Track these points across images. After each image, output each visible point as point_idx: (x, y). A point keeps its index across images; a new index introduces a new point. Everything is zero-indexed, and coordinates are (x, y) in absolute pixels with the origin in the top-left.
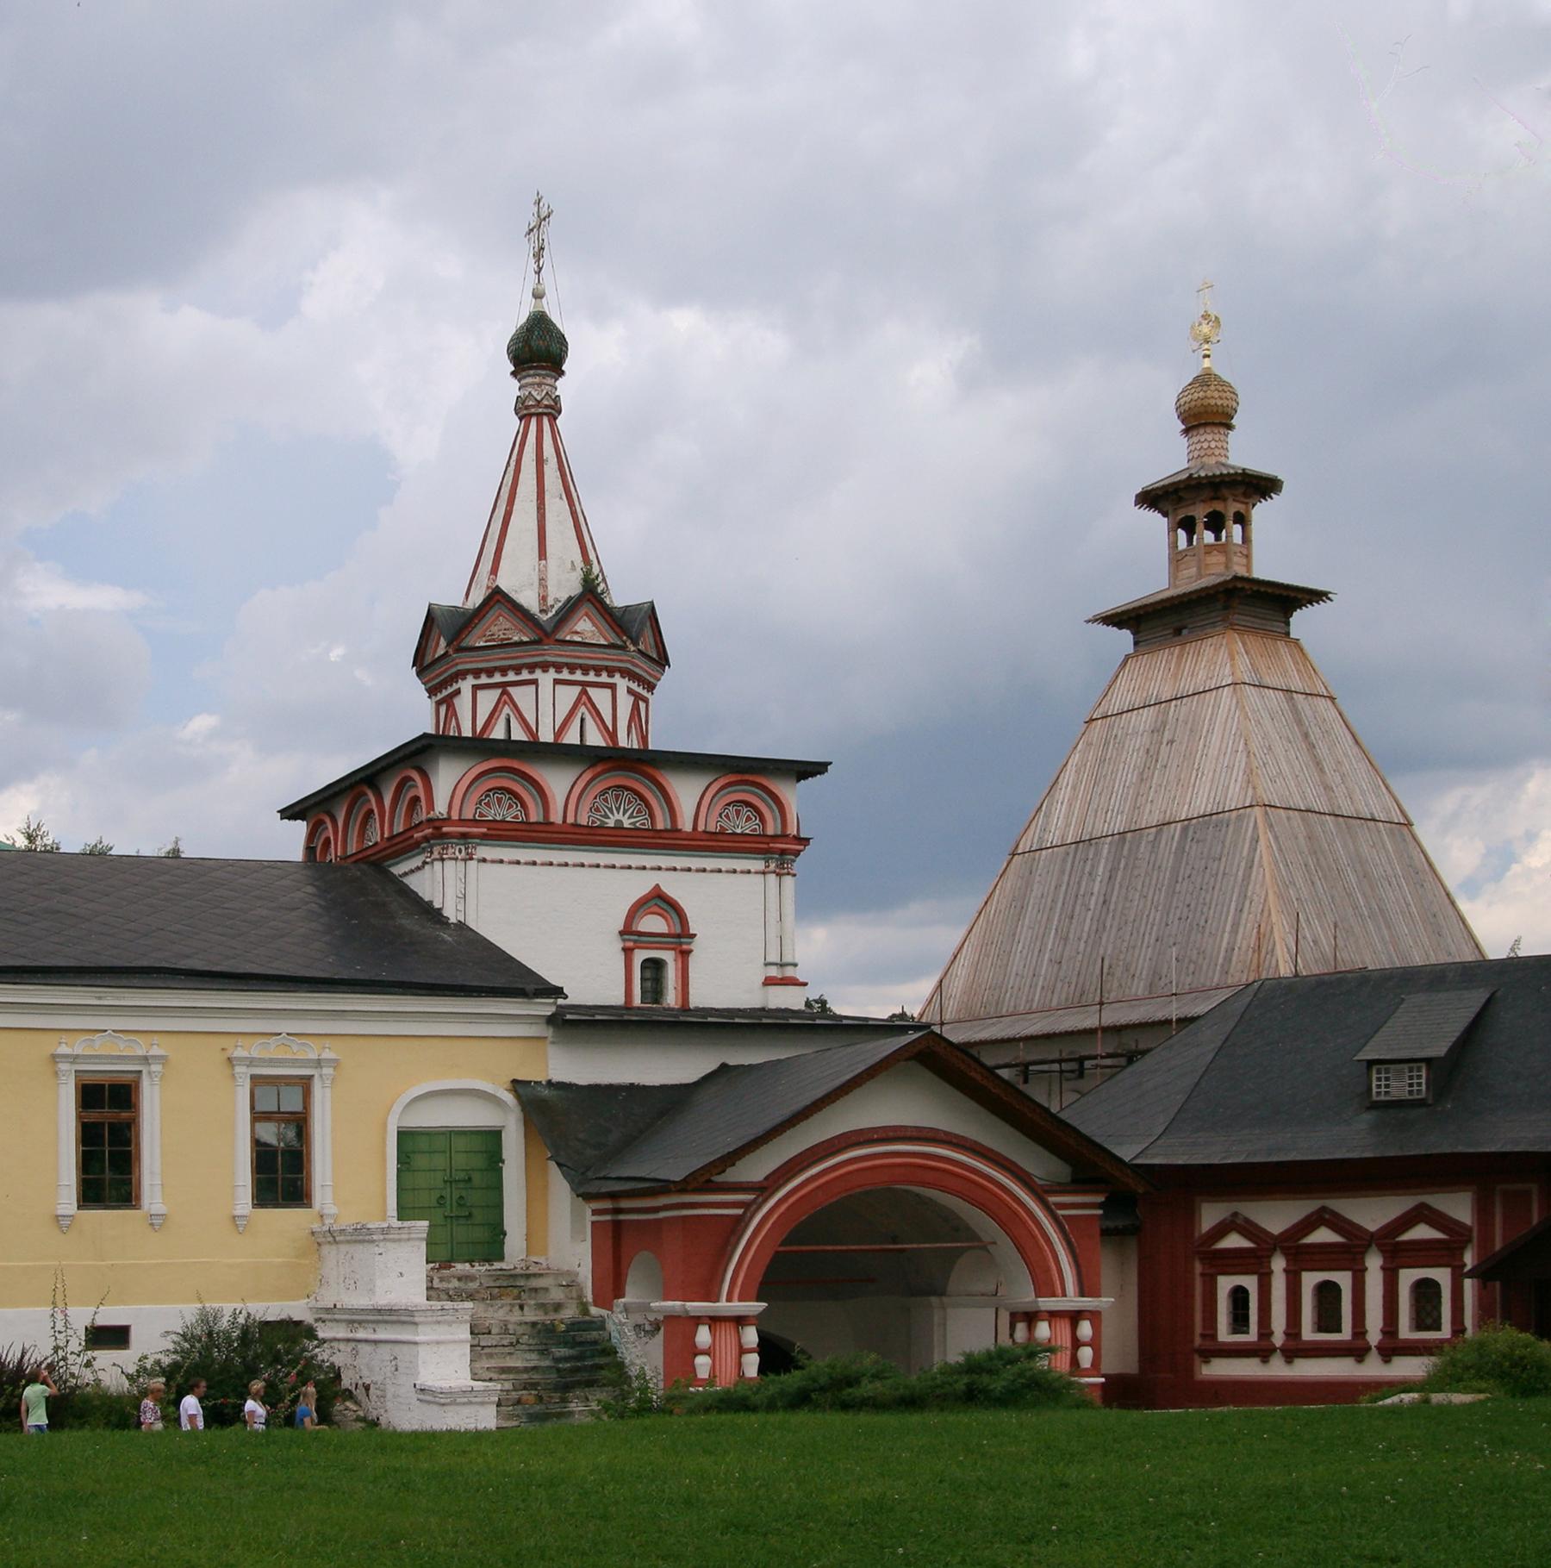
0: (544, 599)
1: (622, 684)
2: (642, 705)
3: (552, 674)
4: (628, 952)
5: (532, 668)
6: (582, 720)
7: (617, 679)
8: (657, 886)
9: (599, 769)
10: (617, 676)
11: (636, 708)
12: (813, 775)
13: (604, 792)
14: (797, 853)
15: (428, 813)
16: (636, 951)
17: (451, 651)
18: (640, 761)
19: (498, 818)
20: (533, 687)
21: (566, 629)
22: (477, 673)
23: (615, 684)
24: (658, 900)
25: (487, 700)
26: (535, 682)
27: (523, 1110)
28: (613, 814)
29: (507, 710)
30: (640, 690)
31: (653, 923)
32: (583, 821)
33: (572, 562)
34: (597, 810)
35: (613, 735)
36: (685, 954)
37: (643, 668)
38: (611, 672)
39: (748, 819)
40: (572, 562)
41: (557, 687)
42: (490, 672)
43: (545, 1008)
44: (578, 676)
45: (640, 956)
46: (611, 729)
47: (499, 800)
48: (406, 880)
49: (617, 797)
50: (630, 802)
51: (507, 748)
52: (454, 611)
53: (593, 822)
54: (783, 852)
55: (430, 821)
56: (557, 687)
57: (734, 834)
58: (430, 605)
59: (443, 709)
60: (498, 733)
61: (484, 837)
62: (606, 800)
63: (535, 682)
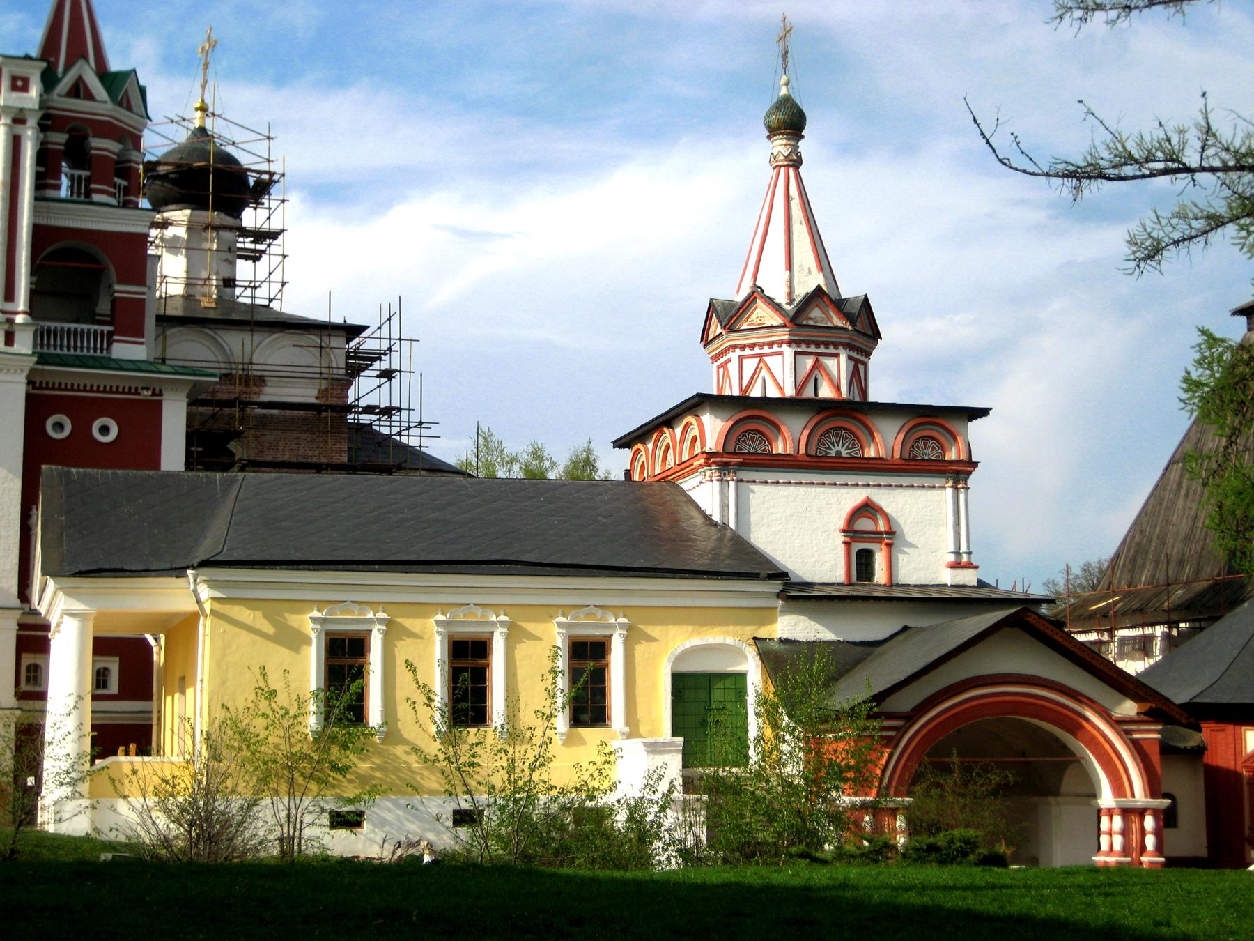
0: (790, 294)
2: (861, 367)
10: (841, 348)
11: (856, 369)
12: (981, 416)
13: (827, 432)
14: (969, 473)
15: (702, 448)
16: (853, 544)
17: (724, 333)
19: (752, 451)
20: (780, 357)
21: (803, 316)
22: (743, 347)
24: (867, 509)
25: (750, 365)
26: (781, 353)
27: (761, 658)
28: (834, 446)
29: (764, 372)
30: (859, 357)
31: (864, 524)
33: (809, 268)
34: (823, 444)
35: (838, 389)
37: (861, 342)
38: (836, 345)
39: (933, 449)
40: (809, 268)
41: (797, 357)
42: (752, 346)
43: (776, 586)
44: (813, 349)
47: (753, 439)
48: (690, 493)
49: (837, 435)
50: (846, 438)
51: (764, 402)
52: (728, 304)
53: (820, 453)
54: (958, 472)
55: (702, 453)
56: (797, 357)
57: (923, 460)
58: (711, 299)
59: (721, 370)
60: (756, 392)
62: (829, 437)
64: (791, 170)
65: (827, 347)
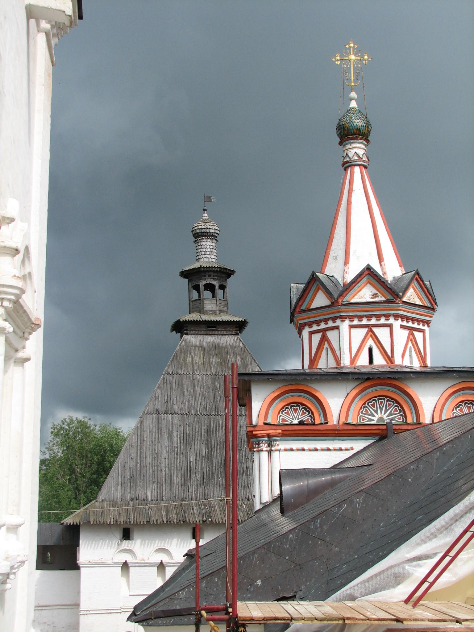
3: (347, 322)
5: (334, 319)
6: (370, 350)
7: (391, 321)
9: (362, 386)
20: (335, 332)
23: (392, 324)
32: (350, 421)
38: (387, 316)
44: (365, 322)
46: (390, 354)
63: (390, 326)
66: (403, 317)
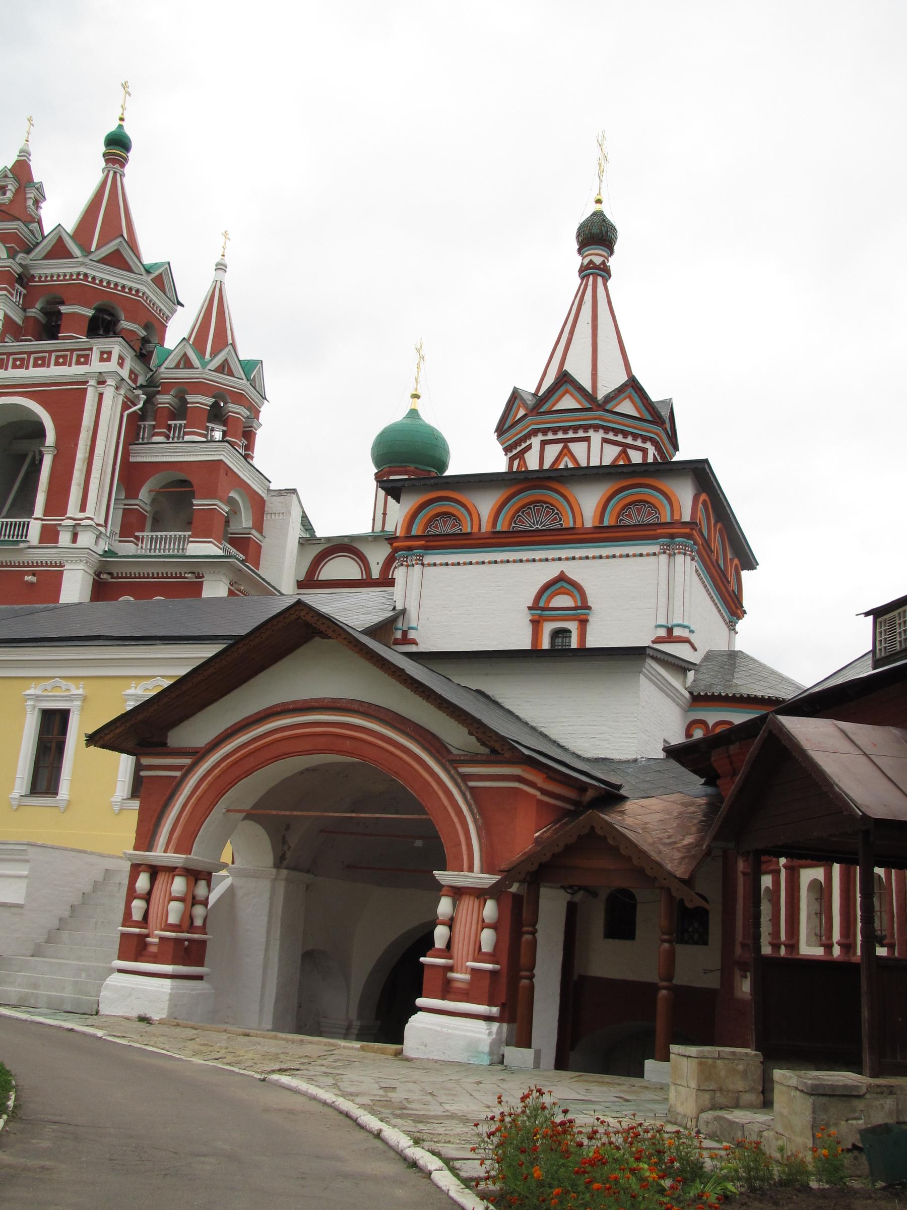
1: (596, 437)
3: (540, 437)
4: (536, 624)
7: (591, 433)
8: (562, 572)
18: (550, 478)
31: (562, 601)
36: (583, 623)
38: (586, 428)
44: (560, 435)
45: (548, 628)
61: (426, 548)
64: (600, 280)
65: (575, 432)
66: (607, 430)
